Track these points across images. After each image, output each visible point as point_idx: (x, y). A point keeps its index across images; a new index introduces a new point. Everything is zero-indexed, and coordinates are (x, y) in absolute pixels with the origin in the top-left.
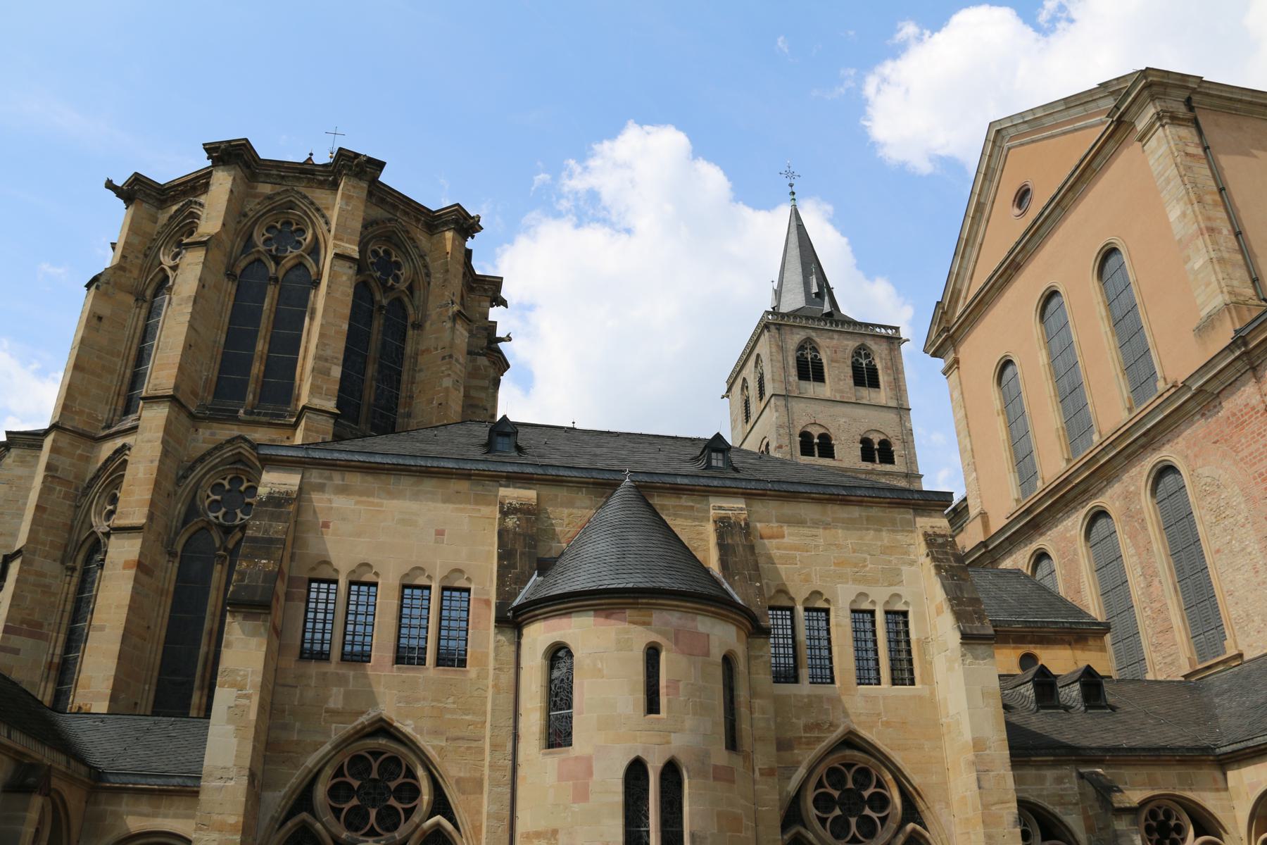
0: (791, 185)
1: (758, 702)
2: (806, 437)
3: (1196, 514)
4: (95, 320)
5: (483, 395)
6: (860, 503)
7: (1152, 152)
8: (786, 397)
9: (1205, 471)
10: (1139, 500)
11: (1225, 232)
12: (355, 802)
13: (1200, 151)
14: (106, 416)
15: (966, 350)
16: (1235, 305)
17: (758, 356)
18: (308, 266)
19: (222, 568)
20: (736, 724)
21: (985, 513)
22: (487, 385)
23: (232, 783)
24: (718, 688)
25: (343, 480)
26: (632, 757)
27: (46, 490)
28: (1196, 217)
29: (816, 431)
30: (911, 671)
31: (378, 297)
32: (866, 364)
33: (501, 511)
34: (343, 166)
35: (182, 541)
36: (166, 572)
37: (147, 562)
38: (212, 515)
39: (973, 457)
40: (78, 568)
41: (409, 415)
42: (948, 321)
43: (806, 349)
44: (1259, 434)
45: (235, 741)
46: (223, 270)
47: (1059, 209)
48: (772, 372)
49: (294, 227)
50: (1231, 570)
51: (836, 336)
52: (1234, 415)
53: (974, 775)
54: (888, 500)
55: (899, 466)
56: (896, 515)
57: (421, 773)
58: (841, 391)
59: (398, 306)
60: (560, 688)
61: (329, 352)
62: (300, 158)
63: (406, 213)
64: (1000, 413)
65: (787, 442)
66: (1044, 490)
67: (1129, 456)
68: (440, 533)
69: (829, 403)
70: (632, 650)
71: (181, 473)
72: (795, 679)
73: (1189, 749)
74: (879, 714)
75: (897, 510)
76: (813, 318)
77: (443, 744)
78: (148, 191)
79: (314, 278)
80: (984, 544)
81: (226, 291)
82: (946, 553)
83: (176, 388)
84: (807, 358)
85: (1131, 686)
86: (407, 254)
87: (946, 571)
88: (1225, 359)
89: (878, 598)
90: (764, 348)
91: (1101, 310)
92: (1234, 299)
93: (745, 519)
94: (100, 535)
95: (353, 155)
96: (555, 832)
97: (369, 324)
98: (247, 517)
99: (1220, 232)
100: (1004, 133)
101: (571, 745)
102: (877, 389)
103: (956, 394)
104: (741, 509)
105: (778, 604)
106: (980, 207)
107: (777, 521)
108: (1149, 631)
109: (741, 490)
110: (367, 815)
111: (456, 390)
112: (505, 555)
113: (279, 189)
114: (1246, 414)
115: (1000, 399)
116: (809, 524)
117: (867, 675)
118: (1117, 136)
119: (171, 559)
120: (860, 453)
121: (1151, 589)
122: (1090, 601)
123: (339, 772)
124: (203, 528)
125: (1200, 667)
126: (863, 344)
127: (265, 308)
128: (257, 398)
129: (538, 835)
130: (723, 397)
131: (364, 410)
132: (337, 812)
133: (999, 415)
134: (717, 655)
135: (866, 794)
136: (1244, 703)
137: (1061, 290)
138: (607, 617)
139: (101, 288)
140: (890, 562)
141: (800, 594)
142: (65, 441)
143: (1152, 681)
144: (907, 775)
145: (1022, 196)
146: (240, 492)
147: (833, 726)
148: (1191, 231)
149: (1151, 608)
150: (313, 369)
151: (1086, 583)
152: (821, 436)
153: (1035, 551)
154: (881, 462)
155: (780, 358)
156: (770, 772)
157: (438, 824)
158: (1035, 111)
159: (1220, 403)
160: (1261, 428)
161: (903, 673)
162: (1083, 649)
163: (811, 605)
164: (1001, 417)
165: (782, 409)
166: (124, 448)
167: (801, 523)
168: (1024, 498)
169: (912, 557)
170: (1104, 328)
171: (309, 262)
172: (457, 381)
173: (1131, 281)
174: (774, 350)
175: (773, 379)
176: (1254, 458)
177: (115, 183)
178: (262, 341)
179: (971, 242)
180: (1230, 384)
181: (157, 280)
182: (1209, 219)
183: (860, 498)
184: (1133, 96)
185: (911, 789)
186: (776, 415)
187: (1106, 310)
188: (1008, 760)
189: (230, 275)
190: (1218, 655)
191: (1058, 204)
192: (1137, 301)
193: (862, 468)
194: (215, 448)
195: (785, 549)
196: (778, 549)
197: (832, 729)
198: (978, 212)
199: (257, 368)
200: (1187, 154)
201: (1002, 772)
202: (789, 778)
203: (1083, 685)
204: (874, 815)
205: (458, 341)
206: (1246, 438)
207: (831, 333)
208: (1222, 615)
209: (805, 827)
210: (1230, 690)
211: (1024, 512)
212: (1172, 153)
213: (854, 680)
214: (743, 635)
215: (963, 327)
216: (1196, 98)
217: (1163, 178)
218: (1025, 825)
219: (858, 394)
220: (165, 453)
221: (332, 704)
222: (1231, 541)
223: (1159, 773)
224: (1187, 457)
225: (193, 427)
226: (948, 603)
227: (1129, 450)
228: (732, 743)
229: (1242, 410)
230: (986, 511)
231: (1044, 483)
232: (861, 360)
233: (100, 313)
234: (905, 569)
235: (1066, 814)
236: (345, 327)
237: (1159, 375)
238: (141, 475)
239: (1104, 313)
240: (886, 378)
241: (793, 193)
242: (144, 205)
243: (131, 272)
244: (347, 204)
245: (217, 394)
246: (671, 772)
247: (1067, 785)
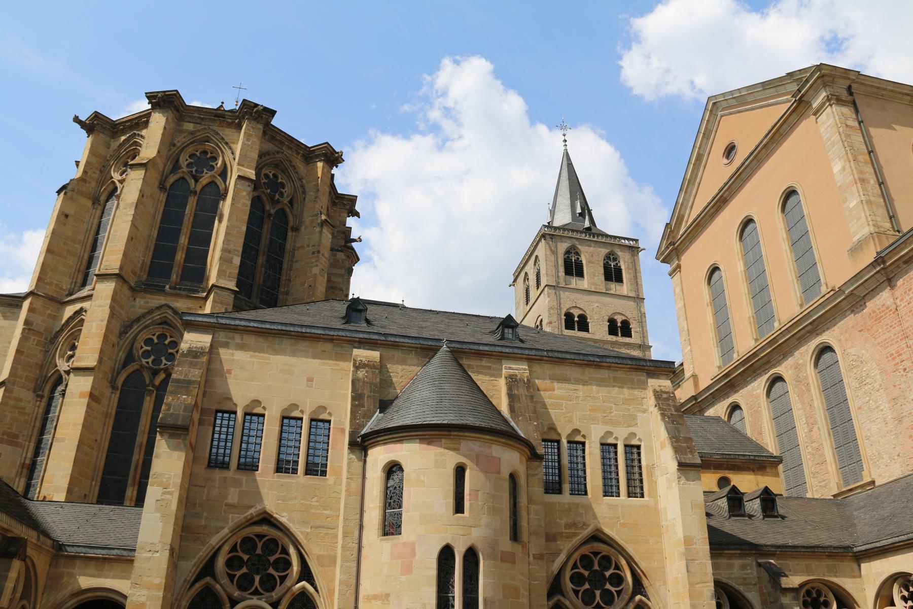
1: (533, 507)
2: (569, 317)
3: (845, 381)
4: (63, 216)
5: (340, 280)
6: (609, 368)
7: (822, 123)
9: (853, 351)
10: (806, 370)
11: (872, 182)
12: (244, 570)
13: (856, 124)
14: (69, 287)
15: (685, 259)
16: (878, 234)
17: (537, 257)
18: (218, 183)
19: (150, 399)
20: (518, 522)
21: (696, 376)
22: (343, 273)
23: (158, 555)
25: (242, 340)
26: (444, 543)
27: (24, 339)
28: (852, 171)
29: (576, 313)
31: (268, 207)
32: (614, 266)
33: (354, 366)
34: (246, 112)
36: (110, 401)
37: (96, 393)
38: (144, 361)
39: (689, 336)
40: (46, 396)
41: (287, 293)
42: (674, 237)
44: (891, 326)
45: (161, 525)
46: (157, 183)
48: (547, 269)
49: (209, 155)
50: (868, 422)
51: (593, 245)
52: (874, 312)
53: (684, 562)
54: (629, 366)
55: (635, 339)
56: (634, 377)
57: (292, 551)
58: (595, 284)
60: (394, 493)
61: (232, 247)
62: (215, 106)
64: (709, 304)
66: (738, 360)
67: (799, 339)
68: (310, 380)
69: (584, 292)
70: (446, 468)
71: (123, 329)
72: (560, 491)
73: (835, 548)
74: (618, 518)
75: (634, 373)
76: (577, 231)
77: (309, 530)
78: (104, 125)
79: (222, 192)
80: (694, 398)
81: (159, 199)
82: (669, 405)
83: (121, 268)
84: (572, 260)
85: (796, 502)
86: (289, 177)
87: (669, 418)
88: (869, 272)
90: (541, 251)
91: (783, 234)
92: (877, 230)
93: (527, 377)
94: (63, 373)
95: (253, 105)
97: (261, 226)
98: (169, 363)
99: (869, 182)
100: (718, 104)
101: (400, 534)
102: (621, 284)
104: (525, 369)
105: (549, 437)
106: (699, 157)
107: (550, 379)
108: (810, 463)
109: (525, 356)
110: (253, 579)
111: (322, 276)
112: (357, 398)
114: (883, 311)
115: (709, 294)
116: (572, 382)
117: (610, 489)
118: (799, 111)
119: (114, 391)
120: (607, 329)
121: (812, 433)
122: (769, 441)
123: (234, 549)
124: (137, 370)
125: (844, 489)
126: (612, 251)
127: (186, 213)
128: (179, 277)
129: (375, 597)
130: (510, 286)
131: (255, 288)
132: (231, 577)
133: (708, 306)
134: (505, 474)
135: (607, 574)
136: (875, 516)
137: (755, 219)
138: (429, 444)
139: (68, 194)
140: (629, 410)
141: (564, 432)
142: (39, 303)
143: (810, 498)
144: (637, 561)
145: (730, 150)
146: (165, 344)
147: (585, 525)
148: (848, 181)
149: (812, 447)
150: (221, 258)
151: (766, 427)
152: (580, 316)
153: (731, 404)
154: (622, 336)
156: (540, 557)
157: (304, 588)
158: (741, 90)
159: (865, 303)
160: (893, 321)
161: (636, 489)
162: (762, 475)
163: (572, 439)
164: (710, 307)
165: (553, 296)
166: (81, 310)
167: (567, 381)
169: (645, 407)
170: (785, 246)
171: (219, 181)
172: (323, 270)
173: (805, 214)
175: (547, 274)
176: (887, 343)
177: (80, 118)
178: (184, 237)
179: (692, 182)
180: (872, 290)
183: (609, 364)
184: (810, 83)
185: (639, 571)
186: (548, 299)
187: (787, 234)
188: (709, 553)
190: (858, 482)
191: (755, 157)
192: (809, 229)
193: (609, 339)
195: (555, 398)
196: (550, 398)
197: (584, 527)
198: (698, 160)
199: (180, 256)
200: (847, 126)
201: (704, 561)
202: (553, 561)
203: (762, 500)
204: (613, 589)
205: (324, 241)
206: (882, 328)
207: (589, 243)
208: (861, 453)
209: (563, 595)
210: (865, 506)
211: (723, 376)
212: (837, 124)
213: (601, 493)
214: (524, 459)
215: (684, 242)
216: (854, 86)
217: (830, 142)
218: (718, 598)
219: (608, 287)
220: (112, 315)
222: (869, 400)
223: (814, 563)
224: (840, 340)
225: (132, 297)
226: (669, 440)
227: (799, 334)
228: (515, 536)
229: (880, 309)
230: (697, 374)
231: (738, 356)
232: (610, 263)
233: (67, 211)
234: (639, 414)
235: (747, 592)
236: (244, 228)
237: (822, 281)
238: (94, 330)
239: (785, 236)
240: (627, 276)
241: (565, 141)
242: (101, 135)
243: (90, 183)
244: (248, 140)
245: (150, 274)
247: (749, 571)
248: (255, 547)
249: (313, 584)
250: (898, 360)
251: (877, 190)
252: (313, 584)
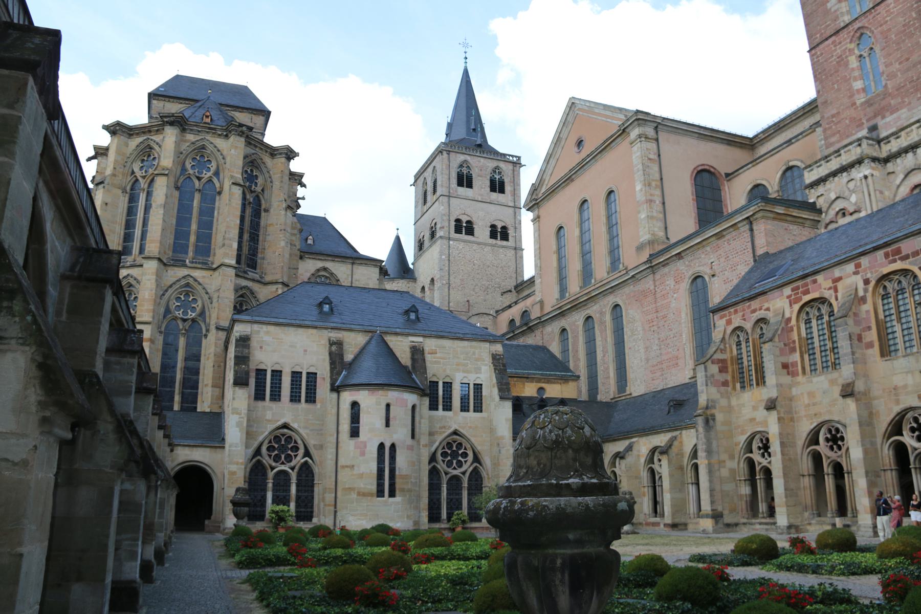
0: (465, 53)
2: (458, 221)
3: (625, 330)
6: (468, 340)
8: (449, 196)
9: (631, 312)
11: (657, 202)
12: (276, 452)
13: (656, 157)
17: (434, 167)
23: (239, 448)
24: (410, 417)
29: (464, 219)
30: (481, 407)
31: (248, 197)
33: (330, 344)
35: (164, 326)
38: (177, 313)
41: (263, 258)
42: (537, 195)
47: (593, 160)
49: (206, 159)
55: (511, 243)
57: (300, 442)
58: (482, 195)
59: (258, 200)
63: (261, 149)
65: (447, 225)
71: (162, 293)
72: (437, 409)
80: (539, 318)
83: (159, 253)
86: (261, 171)
89: (472, 379)
91: (604, 219)
96: (353, 466)
98: (194, 314)
99: (655, 202)
103: (537, 235)
113: (198, 138)
117: (464, 408)
118: (623, 136)
120: (489, 234)
123: (270, 442)
129: (347, 467)
131: (243, 258)
132: (270, 456)
134: (410, 407)
135: (460, 452)
139: (106, 187)
145: (580, 143)
147: (450, 427)
152: (469, 222)
154: (501, 239)
156: (425, 446)
161: (478, 408)
165: (446, 205)
168: (561, 299)
170: (604, 229)
171: (215, 180)
174: (444, 167)
181: (132, 181)
182: (651, 195)
189: (177, 188)
194: (177, 281)
199: (193, 238)
200: (650, 159)
216: (660, 127)
220: (157, 286)
221: (267, 418)
227: (605, 293)
228: (413, 437)
233: (107, 201)
239: (605, 221)
241: (466, 58)
242: (122, 137)
245: (174, 251)
246: (393, 447)
248: (280, 440)
249: (311, 458)
250: (651, 325)
251: (660, 208)
252: (311, 458)
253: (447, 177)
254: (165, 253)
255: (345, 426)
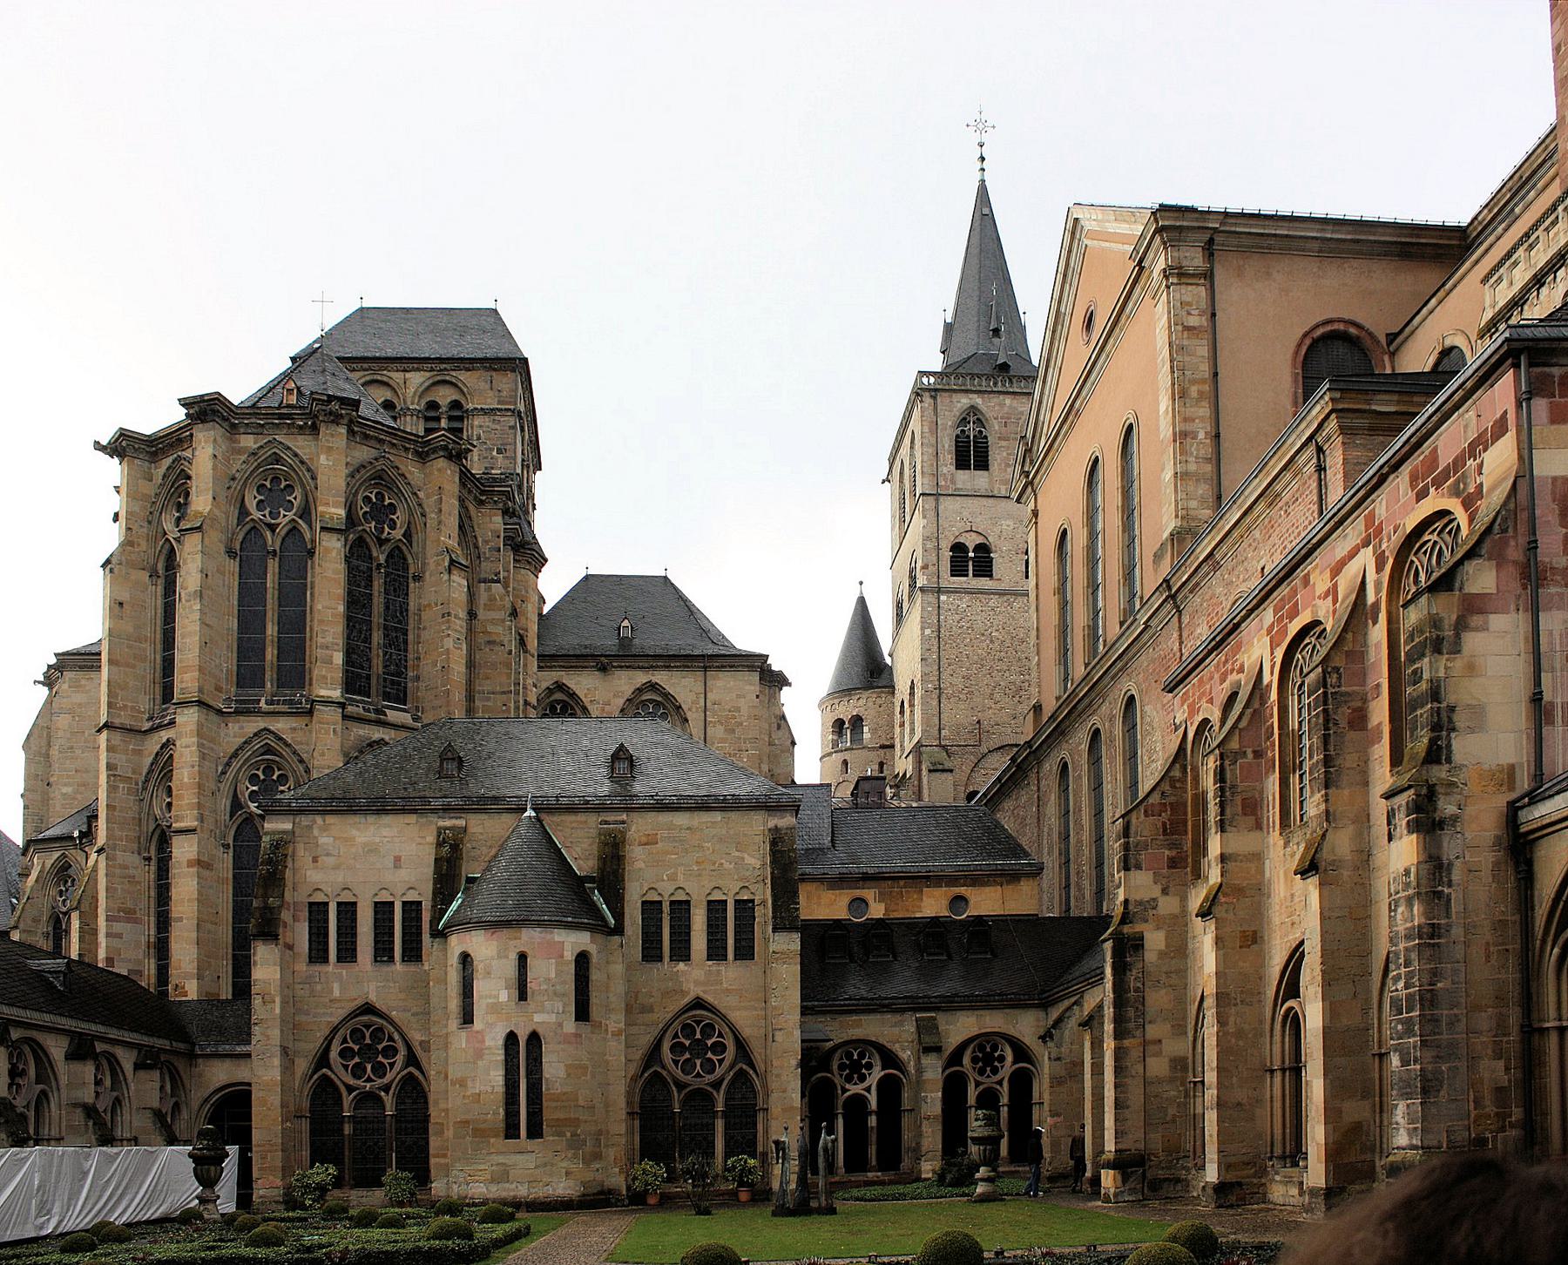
14: (147, 707)
43: (969, 422)
83: (201, 690)
84: (968, 437)
111: (458, 648)
134: (569, 955)
142: (117, 737)
155: (933, 441)
166: (169, 743)
172: (458, 639)
207: (1001, 397)
214: (599, 937)
228: (582, 1013)
245: (239, 685)
246: (534, 1038)
253: (931, 450)
254: (218, 689)
255: (454, 1004)
